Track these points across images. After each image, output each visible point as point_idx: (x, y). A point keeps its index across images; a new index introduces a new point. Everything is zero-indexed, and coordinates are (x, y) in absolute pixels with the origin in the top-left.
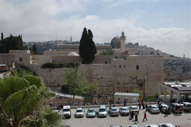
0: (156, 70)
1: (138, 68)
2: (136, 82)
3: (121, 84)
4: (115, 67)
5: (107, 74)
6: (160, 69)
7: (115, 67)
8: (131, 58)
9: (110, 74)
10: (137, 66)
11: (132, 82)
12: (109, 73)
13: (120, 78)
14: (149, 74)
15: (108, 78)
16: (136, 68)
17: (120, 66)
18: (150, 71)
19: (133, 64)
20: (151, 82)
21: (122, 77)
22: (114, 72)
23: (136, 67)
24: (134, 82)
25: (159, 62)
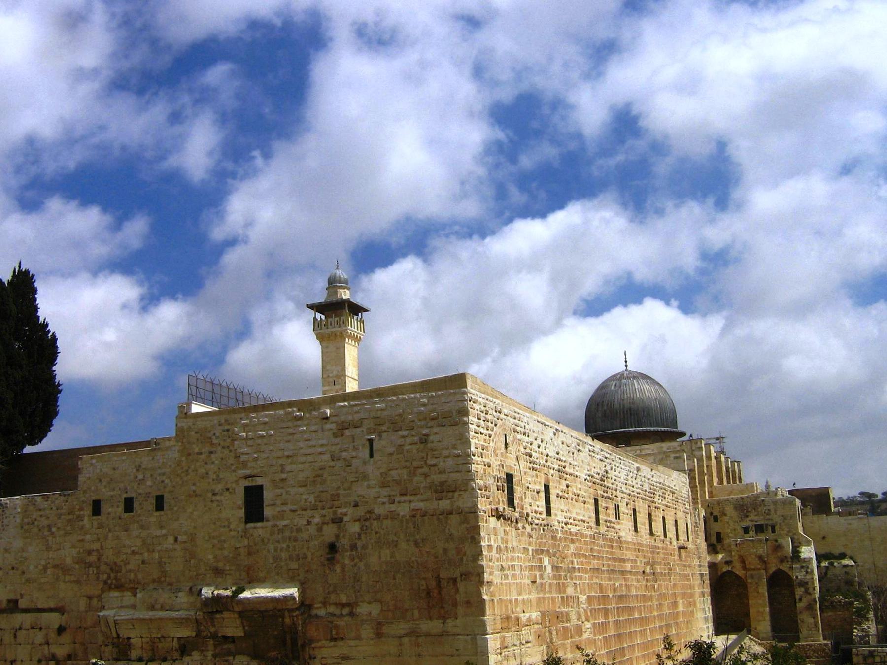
0: (404, 510)
1: (254, 504)
2: (241, 634)
3: (134, 654)
5: (45, 568)
6: (445, 504)
8: (200, 424)
9: (66, 571)
10: (247, 489)
11: (214, 636)
12: (56, 566)
14: (345, 558)
15: (52, 605)
16: (242, 513)
17: (129, 505)
18: (355, 528)
19: (218, 480)
20: (367, 632)
21: (139, 595)
22: (89, 553)
24: (229, 632)
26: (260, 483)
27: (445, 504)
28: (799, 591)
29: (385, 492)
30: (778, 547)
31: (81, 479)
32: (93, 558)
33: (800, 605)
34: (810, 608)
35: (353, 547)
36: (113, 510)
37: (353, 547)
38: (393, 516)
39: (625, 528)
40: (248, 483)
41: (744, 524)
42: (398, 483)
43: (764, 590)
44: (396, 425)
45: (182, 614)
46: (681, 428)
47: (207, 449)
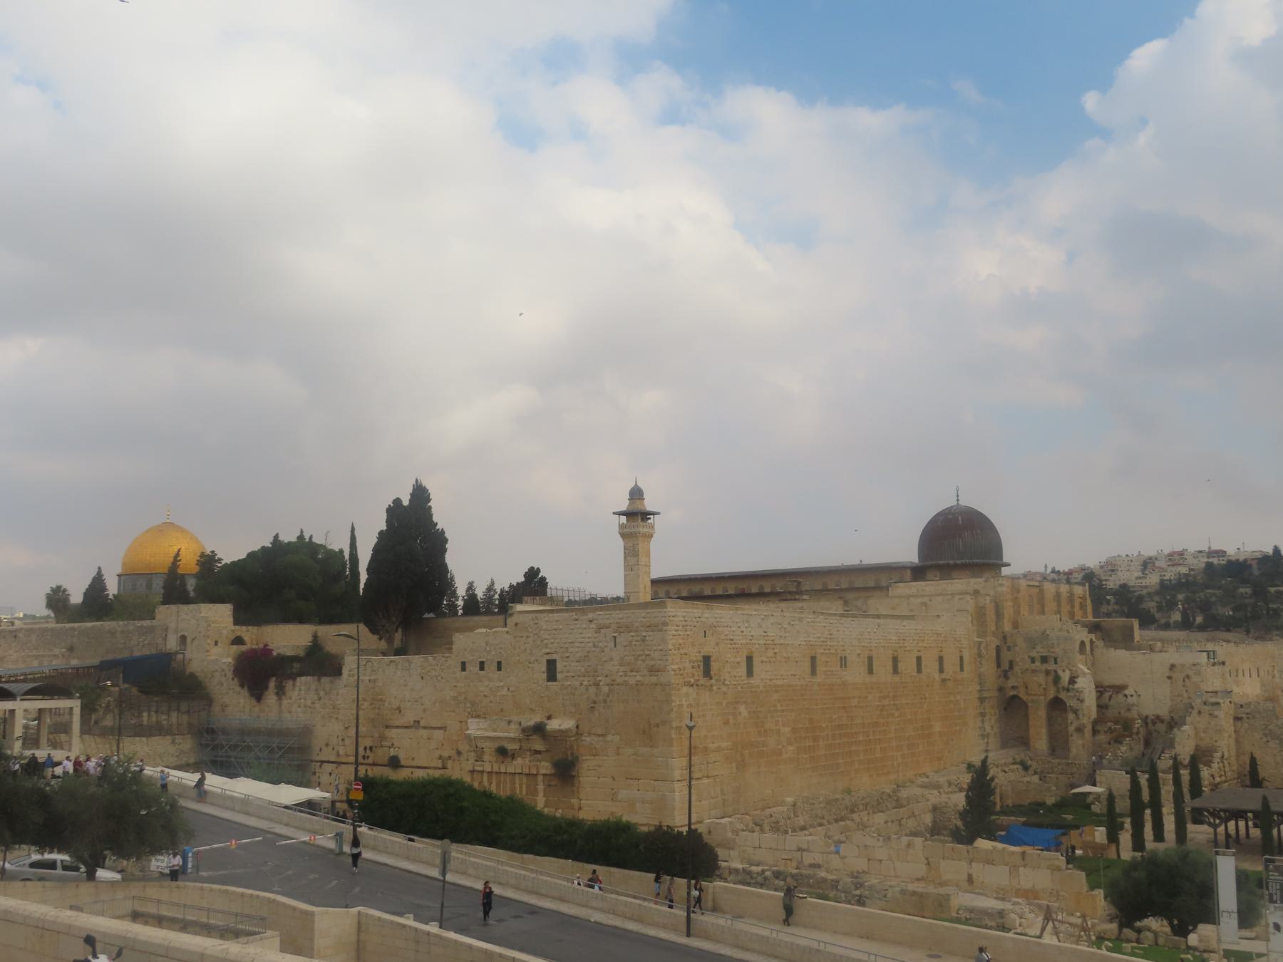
0: (632, 681)
4: (464, 667)
6: (654, 679)
7: (464, 667)
11: (529, 750)
13: (483, 724)
16: (545, 675)
17: (482, 666)
18: (606, 689)
23: (544, 669)
25: (644, 641)
26: (554, 657)
27: (654, 679)
28: (1071, 716)
29: (622, 669)
30: (1057, 679)
31: (454, 647)
32: (461, 698)
33: (1071, 729)
34: (1080, 730)
35: (605, 701)
36: (473, 668)
37: (605, 701)
38: (626, 683)
39: (855, 675)
40: (549, 657)
41: (1034, 654)
42: (629, 664)
43: (1042, 713)
44: (629, 628)
45: (512, 735)
46: (1005, 560)
47: (525, 634)
